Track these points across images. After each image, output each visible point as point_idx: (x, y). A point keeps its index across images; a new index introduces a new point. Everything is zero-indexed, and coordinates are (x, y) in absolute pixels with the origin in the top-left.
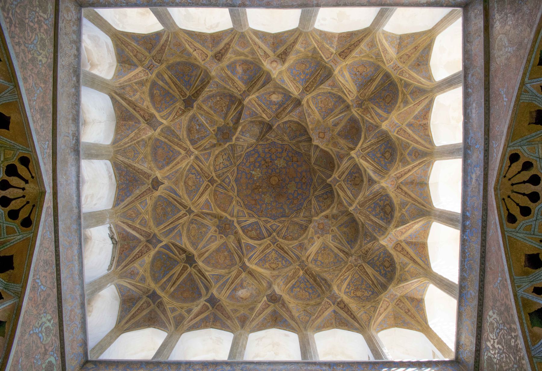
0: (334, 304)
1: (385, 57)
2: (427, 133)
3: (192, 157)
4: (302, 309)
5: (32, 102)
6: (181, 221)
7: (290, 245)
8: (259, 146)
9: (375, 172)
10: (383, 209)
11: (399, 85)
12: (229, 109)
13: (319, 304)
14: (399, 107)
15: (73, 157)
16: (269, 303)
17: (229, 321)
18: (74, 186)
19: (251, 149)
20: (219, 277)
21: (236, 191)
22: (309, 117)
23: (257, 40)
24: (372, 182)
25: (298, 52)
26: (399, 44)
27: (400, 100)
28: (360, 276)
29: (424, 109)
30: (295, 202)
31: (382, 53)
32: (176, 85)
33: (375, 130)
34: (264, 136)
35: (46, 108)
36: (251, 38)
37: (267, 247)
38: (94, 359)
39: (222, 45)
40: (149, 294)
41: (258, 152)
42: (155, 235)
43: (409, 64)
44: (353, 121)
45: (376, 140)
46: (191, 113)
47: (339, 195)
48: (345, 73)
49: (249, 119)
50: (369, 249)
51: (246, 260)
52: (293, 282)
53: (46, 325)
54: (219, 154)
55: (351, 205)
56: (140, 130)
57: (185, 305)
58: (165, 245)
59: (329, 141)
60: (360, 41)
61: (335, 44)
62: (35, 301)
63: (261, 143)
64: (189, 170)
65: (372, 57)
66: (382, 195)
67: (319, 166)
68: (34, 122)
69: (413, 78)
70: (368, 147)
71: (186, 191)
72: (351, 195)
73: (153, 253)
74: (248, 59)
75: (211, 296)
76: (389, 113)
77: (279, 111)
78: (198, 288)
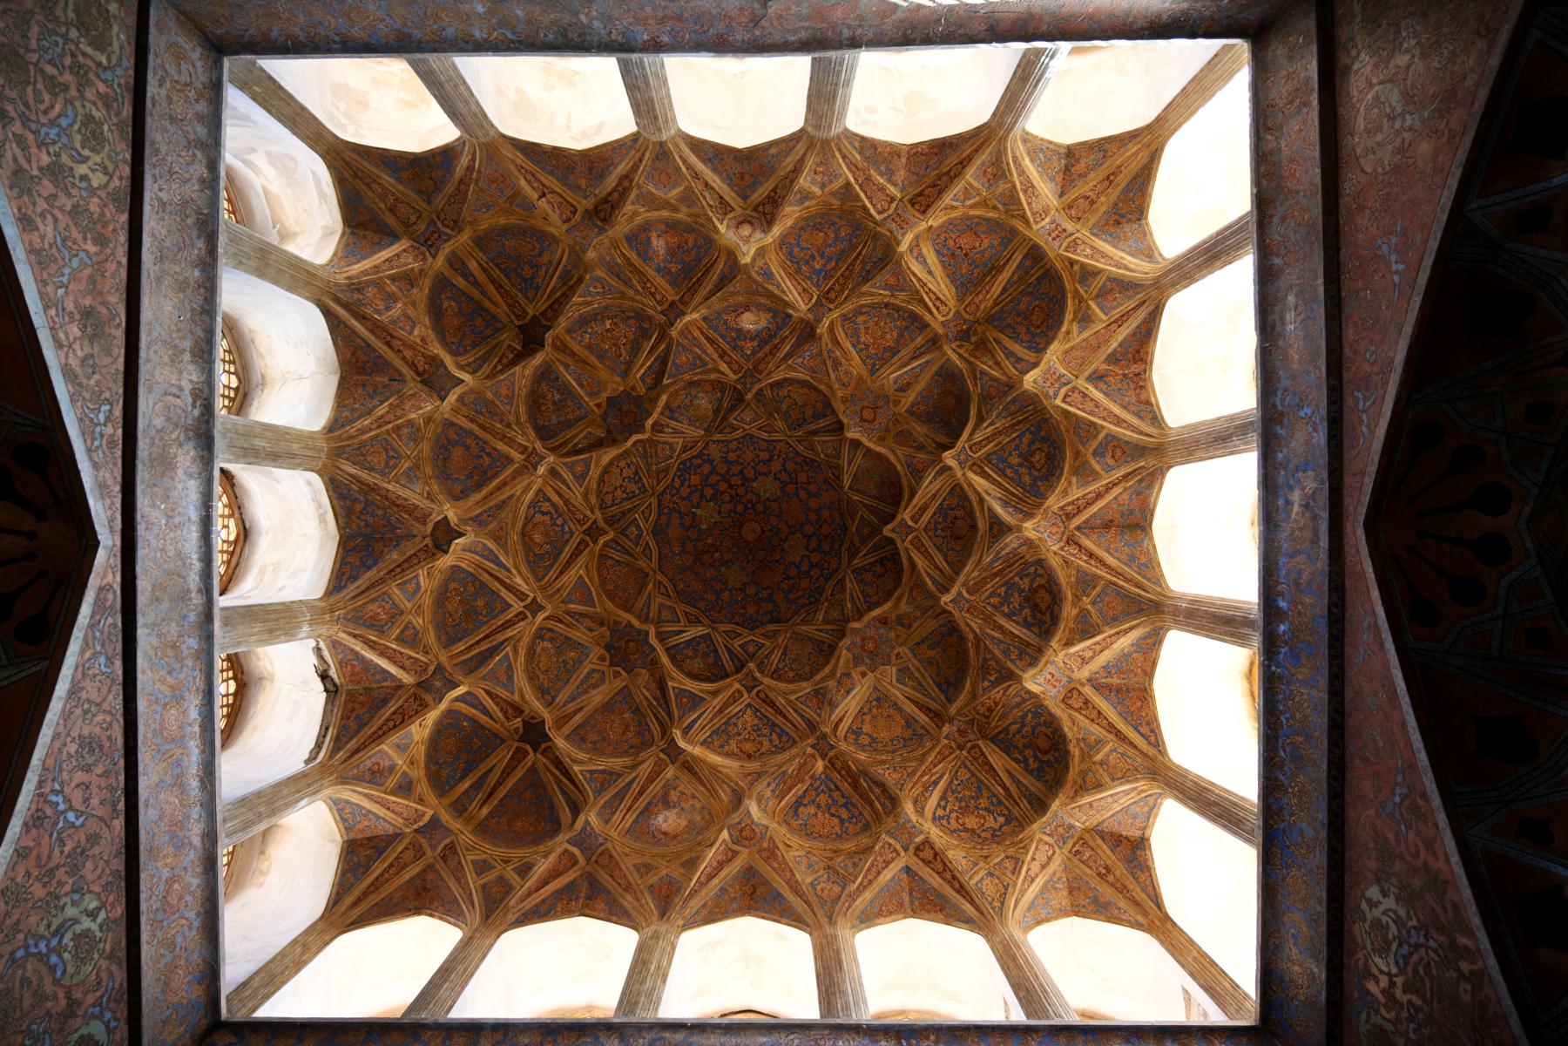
0: (906, 850)
1: (1029, 204)
2: (1143, 397)
3: (541, 470)
4: (822, 865)
5: (50, 289)
6: (509, 633)
7: (791, 694)
8: (713, 447)
9: (1006, 504)
10: (1030, 599)
11: (1065, 276)
12: (635, 349)
13: (868, 850)
14: (1068, 332)
15: (192, 453)
16: (736, 847)
17: (628, 897)
18: (193, 534)
19: (694, 452)
20: (610, 776)
21: (655, 557)
22: (836, 369)
23: (700, 166)
24: (999, 529)
25: (806, 196)
26: (1067, 170)
27: (1069, 316)
28: (973, 775)
29: (1134, 334)
30: (804, 584)
31: (1022, 197)
32: (498, 287)
33: (1005, 394)
34: (724, 419)
35: (104, 311)
36: (685, 161)
37: (733, 699)
38: (240, 1016)
39: (611, 181)
40: (421, 824)
41: (710, 462)
42: (439, 668)
43: (1091, 223)
44: (949, 378)
45: (1007, 422)
46: (538, 360)
47: (913, 566)
48: (925, 251)
49: (687, 377)
50: (996, 704)
51: (677, 733)
52: (798, 790)
53: (78, 929)
54: (611, 463)
55: (947, 590)
56: (402, 399)
57: (517, 853)
58: (468, 693)
59: (887, 429)
60: (964, 164)
61: (901, 175)
62: (39, 857)
64: (533, 504)
65: (995, 208)
67: (864, 493)
68: (59, 345)
69: (1104, 255)
70: (988, 440)
71: (527, 556)
73: (432, 716)
75: (584, 829)
76: (1040, 350)
77: (761, 354)
78: (552, 807)
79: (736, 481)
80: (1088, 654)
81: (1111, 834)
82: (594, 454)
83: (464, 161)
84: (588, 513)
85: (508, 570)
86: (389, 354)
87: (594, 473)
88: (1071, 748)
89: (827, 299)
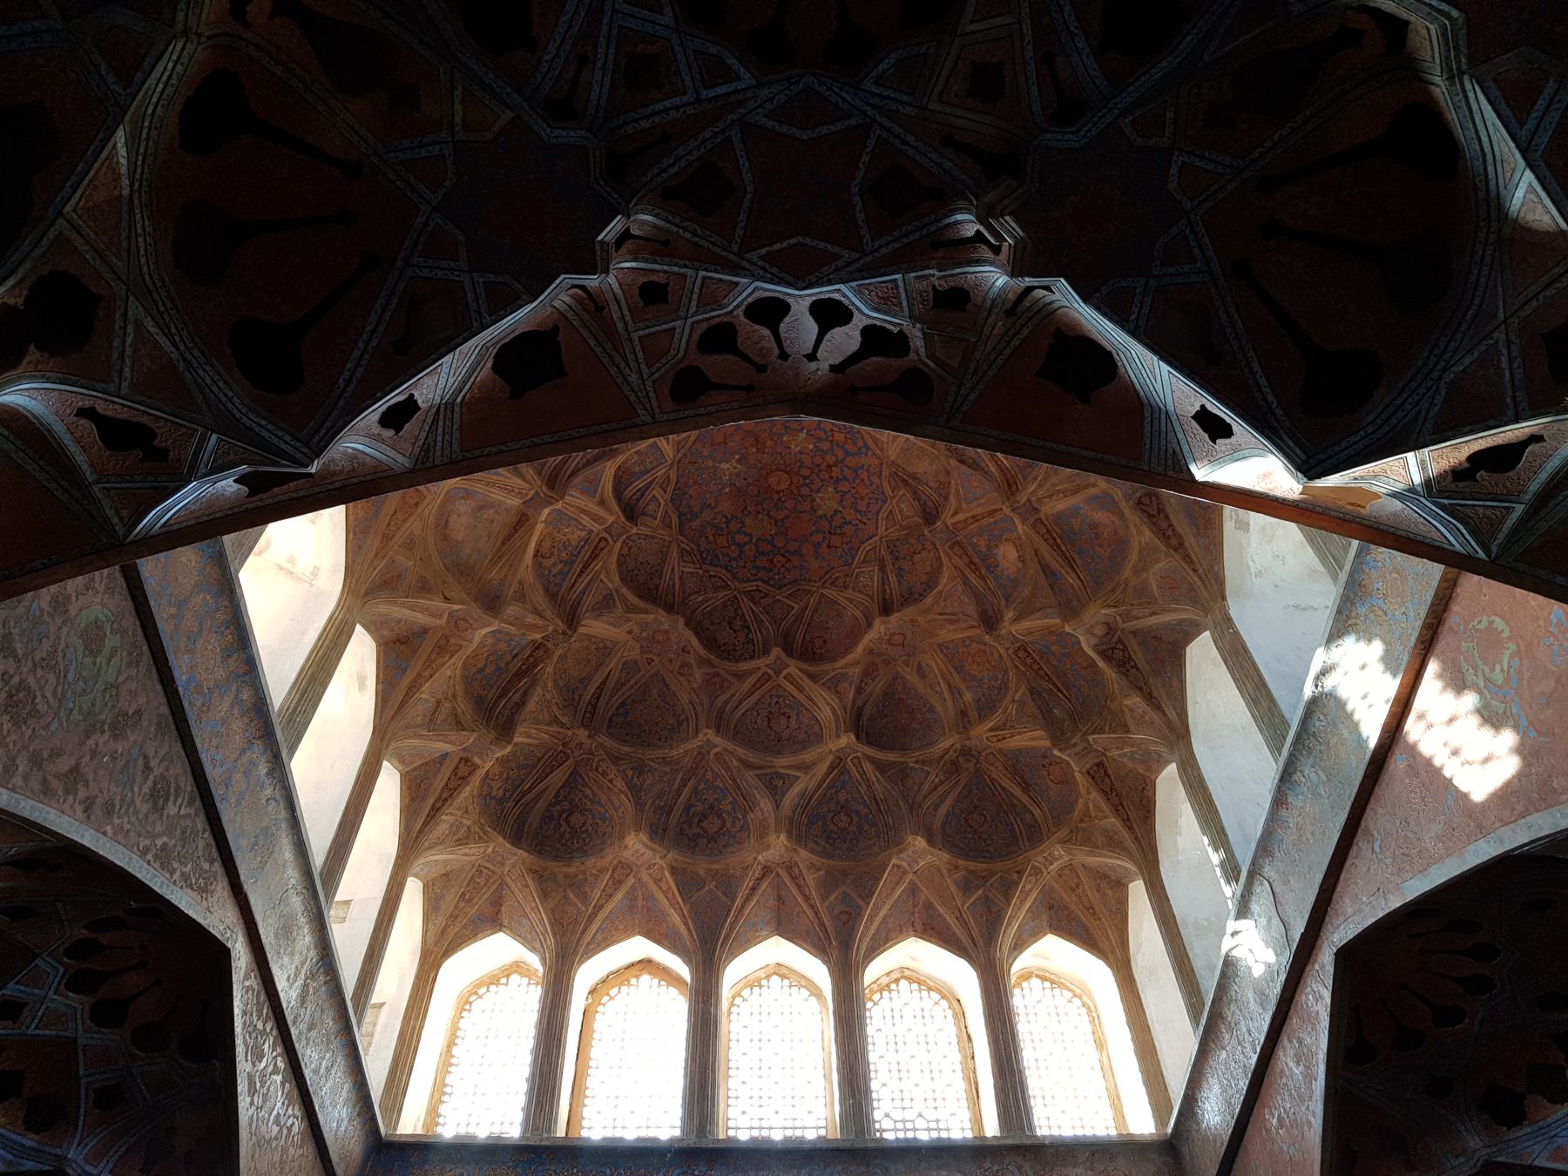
9: (802, 795)
14: (957, 867)
19: (872, 446)
27: (972, 866)
34: (905, 482)
47: (740, 676)
50: (611, 781)
60: (1127, 821)
63: (885, 472)
72: (742, 709)
77: (971, 552)
79: (836, 472)
81: (501, 897)
89: (1022, 649)
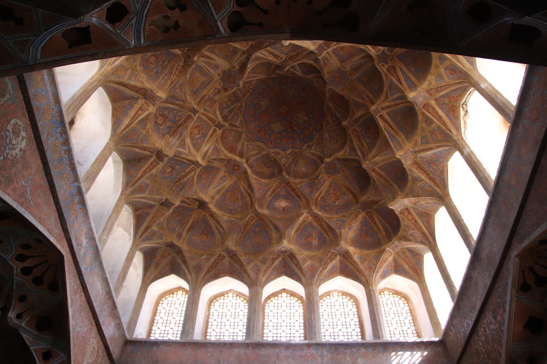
6: (389, 104)
9: (180, 153)
12: (328, 193)
19: (306, 145)
23: (298, 272)
32: (375, 223)
36: (304, 275)
39: (330, 266)
45: (182, 181)
48: (219, 235)
50: (175, 73)
60: (208, 272)
63: (297, 150)
65: (195, 254)
66: (169, 133)
67: (236, 131)
70: (189, 173)
74: (306, 253)
80: (140, 112)
82: (346, 157)
83: (379, 274)
84: (351, 133)
85: (385, 129)
86: (417, 218)
87: (347, 148)
88: (141, 68)
